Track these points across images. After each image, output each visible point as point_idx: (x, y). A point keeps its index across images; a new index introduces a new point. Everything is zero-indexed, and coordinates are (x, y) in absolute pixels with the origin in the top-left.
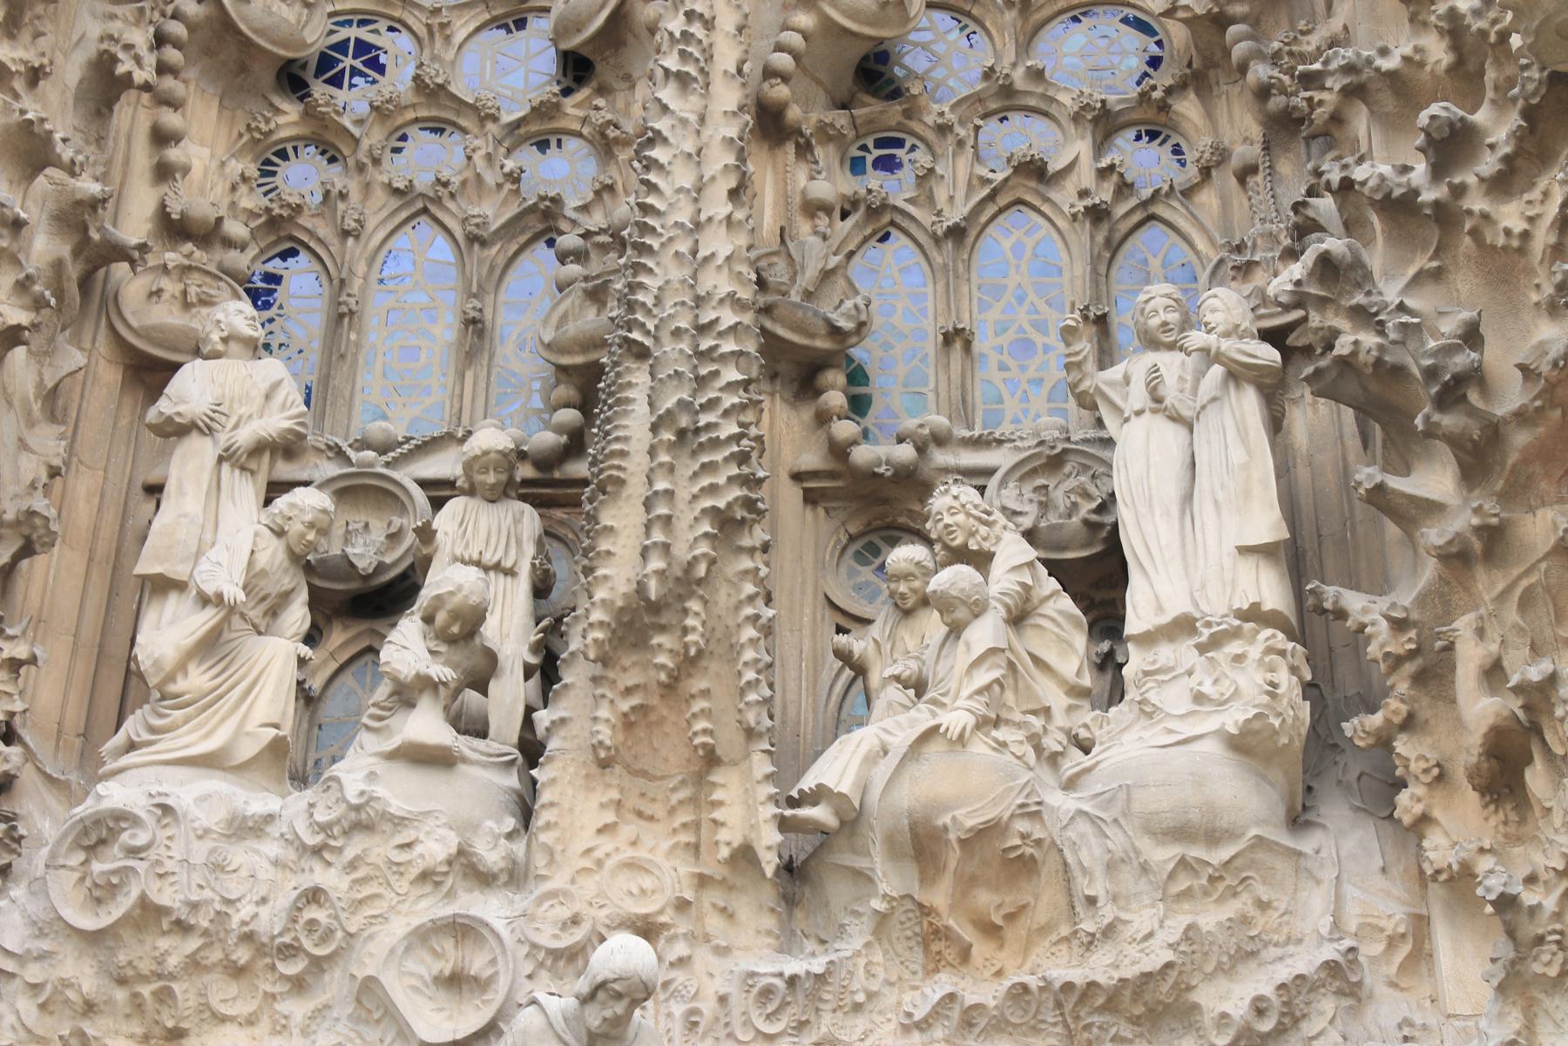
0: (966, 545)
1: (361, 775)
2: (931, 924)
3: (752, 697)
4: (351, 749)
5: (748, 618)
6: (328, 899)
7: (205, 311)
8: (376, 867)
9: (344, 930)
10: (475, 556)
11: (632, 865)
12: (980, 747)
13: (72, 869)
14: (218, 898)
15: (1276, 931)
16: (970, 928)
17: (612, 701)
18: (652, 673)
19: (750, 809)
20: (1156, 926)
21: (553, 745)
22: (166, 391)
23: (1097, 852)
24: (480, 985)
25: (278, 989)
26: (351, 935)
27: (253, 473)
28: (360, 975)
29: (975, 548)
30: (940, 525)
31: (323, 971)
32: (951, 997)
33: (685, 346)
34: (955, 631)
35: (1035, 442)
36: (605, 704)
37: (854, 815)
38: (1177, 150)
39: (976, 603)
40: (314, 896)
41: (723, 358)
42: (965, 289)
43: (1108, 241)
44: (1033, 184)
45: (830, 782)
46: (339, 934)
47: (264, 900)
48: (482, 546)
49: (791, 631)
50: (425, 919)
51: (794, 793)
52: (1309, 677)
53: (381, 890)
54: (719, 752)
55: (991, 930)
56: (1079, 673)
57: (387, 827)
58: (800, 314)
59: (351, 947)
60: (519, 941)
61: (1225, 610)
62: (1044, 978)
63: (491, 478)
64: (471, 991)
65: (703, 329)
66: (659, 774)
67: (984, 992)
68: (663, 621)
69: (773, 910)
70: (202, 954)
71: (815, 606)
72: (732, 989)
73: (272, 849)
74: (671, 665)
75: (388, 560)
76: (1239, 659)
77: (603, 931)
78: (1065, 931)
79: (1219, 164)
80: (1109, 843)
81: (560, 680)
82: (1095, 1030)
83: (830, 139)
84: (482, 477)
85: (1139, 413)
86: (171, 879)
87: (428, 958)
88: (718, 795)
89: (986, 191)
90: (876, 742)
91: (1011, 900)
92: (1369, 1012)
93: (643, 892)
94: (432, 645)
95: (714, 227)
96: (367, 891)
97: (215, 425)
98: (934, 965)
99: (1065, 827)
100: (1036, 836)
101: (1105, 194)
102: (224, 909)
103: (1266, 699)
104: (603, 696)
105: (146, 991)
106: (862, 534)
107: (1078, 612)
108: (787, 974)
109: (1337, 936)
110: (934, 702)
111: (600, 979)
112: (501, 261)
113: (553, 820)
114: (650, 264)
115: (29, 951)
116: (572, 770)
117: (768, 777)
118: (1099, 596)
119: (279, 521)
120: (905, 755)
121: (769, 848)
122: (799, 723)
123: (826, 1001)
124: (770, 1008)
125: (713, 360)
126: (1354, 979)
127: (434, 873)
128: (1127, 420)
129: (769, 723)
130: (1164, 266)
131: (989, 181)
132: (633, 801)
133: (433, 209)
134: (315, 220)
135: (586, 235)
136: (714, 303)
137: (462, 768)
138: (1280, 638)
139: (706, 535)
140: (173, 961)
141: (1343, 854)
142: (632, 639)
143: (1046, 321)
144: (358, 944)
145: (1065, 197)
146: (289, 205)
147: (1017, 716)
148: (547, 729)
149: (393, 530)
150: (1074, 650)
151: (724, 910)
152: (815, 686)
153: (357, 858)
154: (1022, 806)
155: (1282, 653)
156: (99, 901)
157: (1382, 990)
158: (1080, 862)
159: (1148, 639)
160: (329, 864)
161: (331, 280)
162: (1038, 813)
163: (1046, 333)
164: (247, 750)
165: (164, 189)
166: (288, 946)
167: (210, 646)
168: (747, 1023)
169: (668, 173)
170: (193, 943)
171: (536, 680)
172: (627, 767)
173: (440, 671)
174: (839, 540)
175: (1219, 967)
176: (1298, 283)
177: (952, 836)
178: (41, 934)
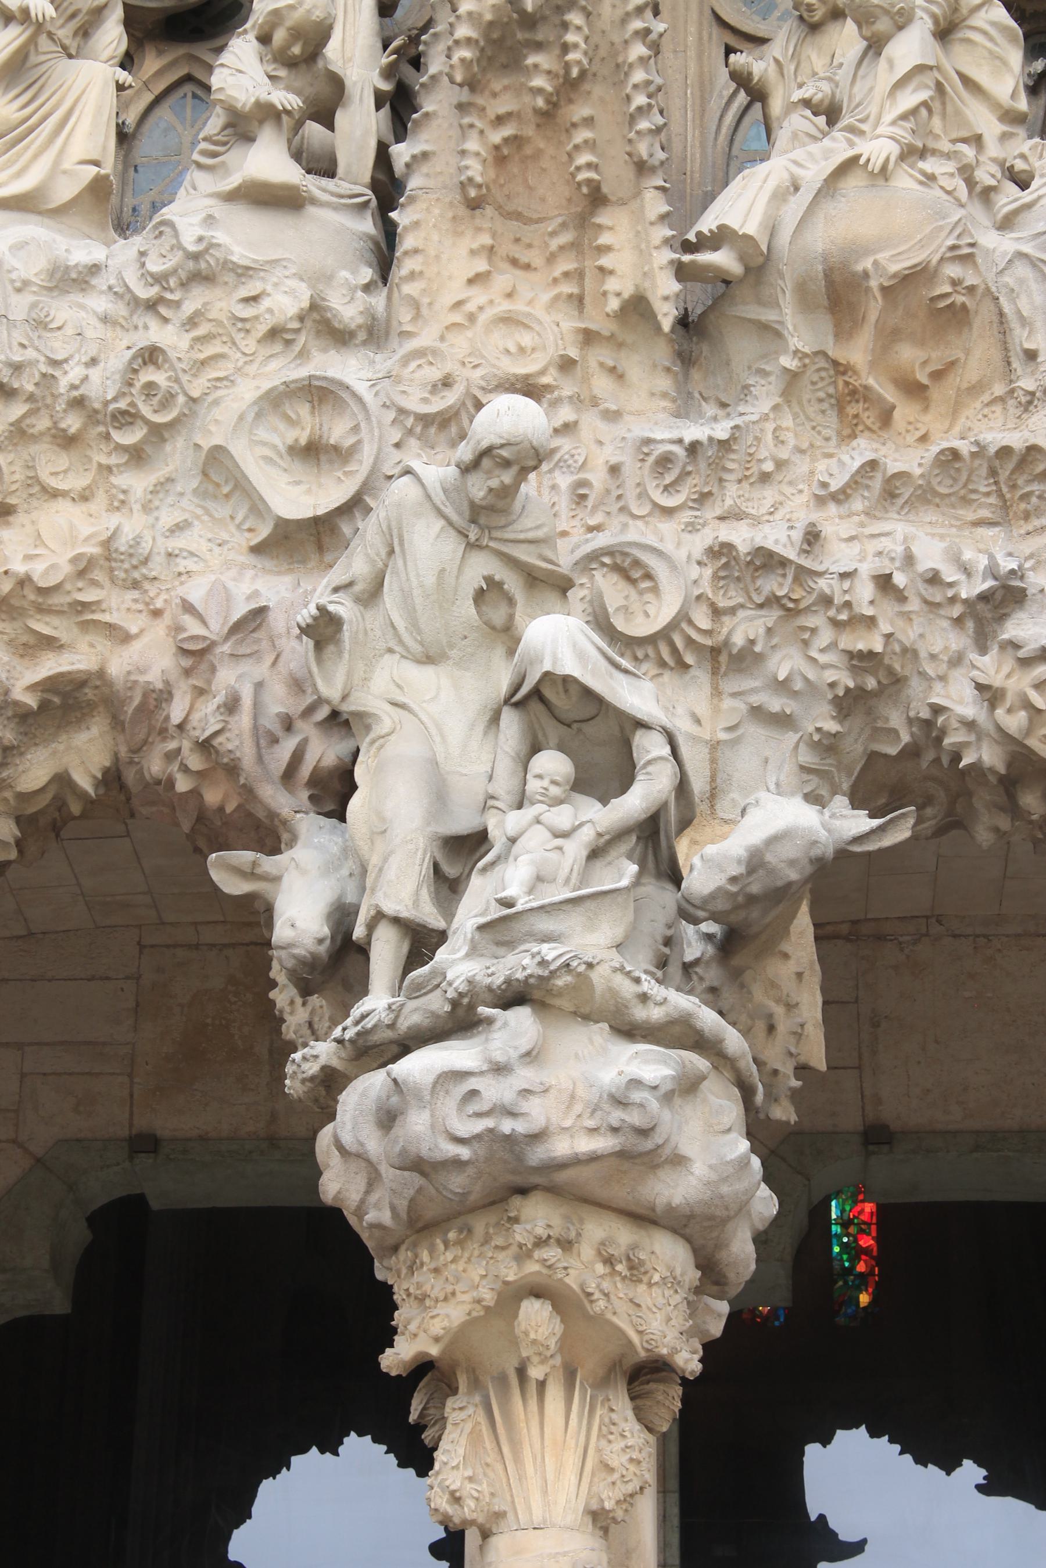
1: (197, 219)
2: (847, 383)
3: (644, 125)
4: (182, 192)
5: (637, 33)
8: (219, 323)
9: (186, 394)
11: (508, 320)
12: (905, 181)
14: (42, 359)
17: (482, 132)
18: (527, 99)
19: (643, 254)
24: (341, 455)
25: (114, 460)
26: (194, 400)
28: (206, 444)
31: (164, 440)
32: (873, 464)
34: (875, 46)
36: (474, 134)
37: (761, 260)
39: (901, 12)
40: (151, 356)
45: (733, 222)
46: (181, 399)
47: (93, 362)
49: (675, 51)
50: (277, 382)
51: (691, 237)
53: (225, 349)
54: (605, 189)
55: (915, 390)
56: (1014, 96)
57: (230, 278)
59: (194, 413)
60: (384, 405)
62: (977, 443)
64: (331, 462)
66: (535, 216)
68: (540, 37)
69: (668, 370)
70: (28, 421)
71: (701, 24)
72: (626, 458)
73: (100, 303)
74: (549, 89)
77: (479, 394)
78: (999, 390)
82: (1034, 500)
87: (282, 426)
88: (604, 239)
90: (786, 176)
91: (938, 357)
93: (522, 350)
94: (270, 68)
96: (209, 350)
98: (850, 431)
100: (968, 283)
102: (50, 371)
104: (471, 126)
107: (1014, 24)
108: (687, 440)
110: (851, 129)
111: (485, 444)
113: (418, 268)
116: (437, 211)
117: (663, 218)
120: (819, 191)
121: (666, 298)
122: (685, 159)
123: (730, 471)
124: (669, 479)
127: (288, 331)
129: (662, 155)
132: (507, 248)
137: (311, 210)
142: (503, 59)
144: (202, 410)
147: (945, 146)
150: (1010, 70)
151: (613, 370)
152: (702, 116)
153: (197, 313)
154: (953, 248)
158: (1019, 312)
160: (166, 320)
164: (66, 191)
166: (124, 413)
168: (643, 495)
171: (386, 110)
172: (499, 208)
173: (285, 98)
177: (874, 283)
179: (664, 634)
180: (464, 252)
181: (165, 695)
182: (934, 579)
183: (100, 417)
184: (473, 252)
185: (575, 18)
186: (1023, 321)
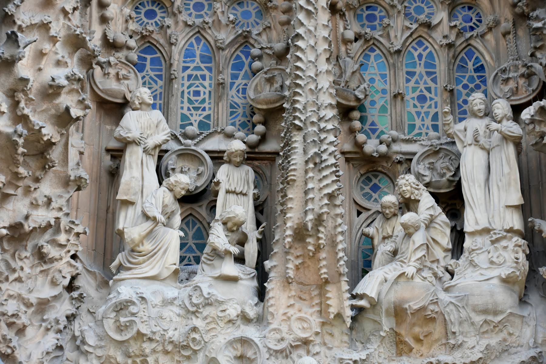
0: (410, 197)
2: (399, 339)
3: (342, 262)
5: (339, 233)
6: (199, 330)
7: (126, 82)
8: (213, 318)
9: (204, 341)
10: (233, 190)
13: (112, 318)
15: (514, 343)
16: (412, 340)
19: (341, 301)
20: (476, 344)
21: (271, 275)
22: (121, 123)
23: (456, 316)
25: (181, 359)
26: (206, 342)
27: (152, 155)
29: (413, 198)
30: (401, 190)
31: (197, 354)
33: (315, 129)
35: (429, 143)
36: (291, 262)
39: (417, 227)
40: (195, 329)
41: (328, 131)
42: (401, 74)
43: (454, 56)
44: (426, 30)
45: (368, 293)
46: (203, 342)
47: (176, 329)
48: (236, 186)
52: (528, 252)
54: (329, 279)
55: (418, 340)
56: (448, 244)
57: (217, 304)
58: (346, 93)
61: (501, 229)
63: (238, 159)
65: (320, 119)
66: (307, 284)
69: (347, 334)
73: (177, 310)
75: (199, 185)
76: (505, 248)
78: (444, 341)
79: (495, 26)
80: (461, 315)
81: (273, 251)
83: (351, 9)
84: (235, 159)
85: (470, 145)
86: (146, 323)
87: (232, 350)
88: (329, 295)
89: (408, 33)
90: (383, 277)
93: (304, 328)
94: (226, 233)
95: (322, 74)
97: (141, 142)
99: (445, 307)
100: (436, 310)
101: (452, 38)
103: (515, 265)
106: (365, 174)
109: (535, 346)
110: (402, 261)
112: (229, 55)
114: (301, 92)
115: (97, 345)
116: (279, 284)
118: (450, 202)
119: (172, 187)
121: (348, 317)
125: (324, 132)
126: (541, 361)
127: (233, 320)
128: (465, 146)
130: (473, 65)
131: (410, 28)
133: (202, 32)
134: (158, 35)
135: (262, 49)
136: (323, 108)
137: (240, 282)
138: (522, 242)
139: (326, 204)
141: (537, 315)
143: (430, 88)
145: (437, 35)
146: (149, 31)
148: (270, 269)
149: (199, 172)
151: (330, 334)
152: (351, 235)
153: (208, 315)
154: (432, 300)
155: (520, 246)
156: (122, 330)
158: (450, 320)
159: (473, 234)
160: (198, 317)
161: (166, 61)
162: (437, 302)
163: (430, 93)
165: (105, 27)
166: (185, 346)
167: (150, 234)
169: (305, 53)
170: (154, 345)
174: (357, 176)
175: (496, 357)
176: (532, 116)
177: (409, 312)
180: (286, 297)
183: (178, 346)
184: (289, 297)
185: (322, 229)
186: (452, 323)
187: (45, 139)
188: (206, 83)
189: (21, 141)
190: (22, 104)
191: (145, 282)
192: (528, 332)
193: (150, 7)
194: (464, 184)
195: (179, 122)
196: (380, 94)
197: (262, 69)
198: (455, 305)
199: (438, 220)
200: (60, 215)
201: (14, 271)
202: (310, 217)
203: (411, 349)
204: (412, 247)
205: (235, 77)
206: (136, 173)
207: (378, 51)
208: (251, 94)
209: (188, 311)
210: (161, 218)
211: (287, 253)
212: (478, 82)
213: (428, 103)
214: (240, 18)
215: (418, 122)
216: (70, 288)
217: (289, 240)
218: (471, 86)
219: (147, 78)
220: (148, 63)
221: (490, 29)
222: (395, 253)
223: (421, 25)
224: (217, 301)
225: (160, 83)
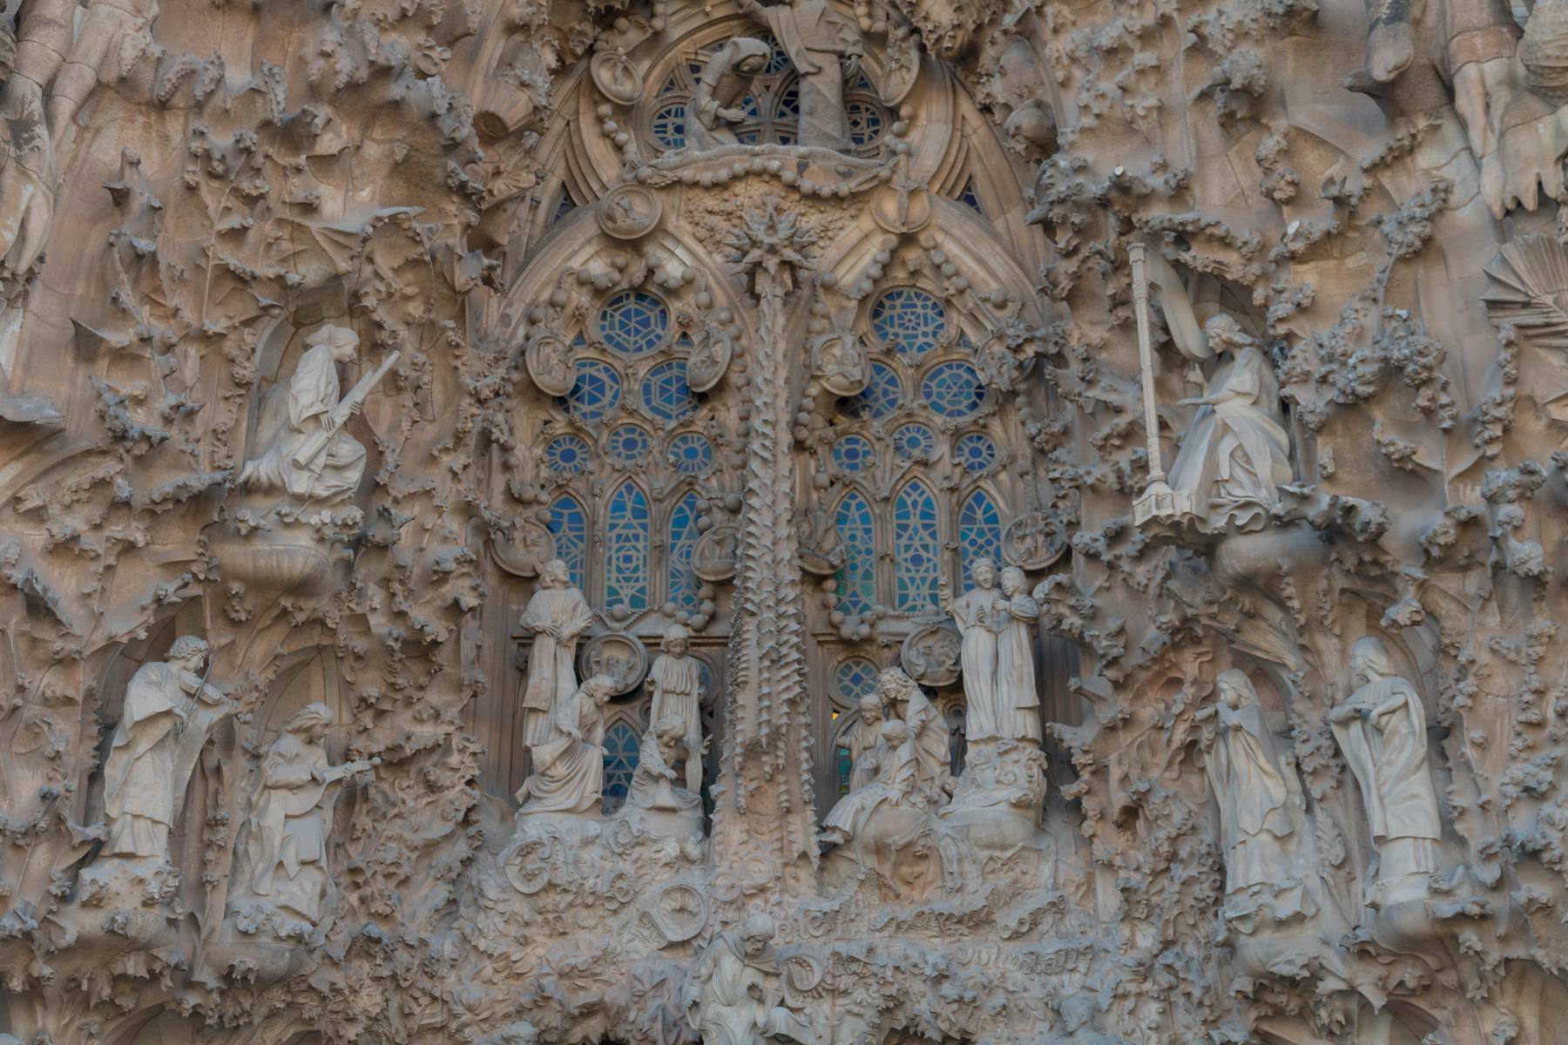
7: (536, 549)
11: (755, 860)
21: (719, 804)
38: (990, 447)
40: (620, 876)
52: (1046, 766)
55: (909, 883)
63: (678, 650)
65: (779, 602)
67: (906, 913)
78: (939, 883)
88: (791, 828)
89: (898, 475)
91: (917, 869)
92: (1067, 921)
96: (642, 872)
101: (956, 479)
105: (551, 917)
140: (562, 906)
145: (937, 474)
157: (1072, 906)
159: (975, 742)
164: (587, 804)
165: (508, 476)
168: (806, 930)
170: (570, 898)
178: (504, 891)
179: (815, 988)
181: (627, 1009)
182: (916, 966)
185: (781, 745)
187: (429, 639)
188: (640, 546)
189: (397, 646)
190: (399, 598)
191: (559, 816)
192: (1046, 870)
193: (568, 446)
194: (966, 677)
195: (606, 598)
196: (864, 555)
197: (711, 526)
198: (953, 839)
199: (933, 725)
200: (451, 729)
201: (394, 805)
202: (765, 730)
203: (898, 896)
204: (897, 764)
205: (677, 536)
206: (547, 672)
207: (861, 498)
208: (696, 560)
209: (614, 853)
210: (577, 734)
211: (738, 775)
212: (989, 536)
213: (925, 565)
214: (683, 459)
215: (912, 591)
216: (466, 822)
217: (739, 759)
218: (981, 541)
219: (564, 540)
220: (565, 520)
221: (1004, 467)
222: (876, 770)
223: (916, 463)
224: (649, 839)
225: (581, 546)
